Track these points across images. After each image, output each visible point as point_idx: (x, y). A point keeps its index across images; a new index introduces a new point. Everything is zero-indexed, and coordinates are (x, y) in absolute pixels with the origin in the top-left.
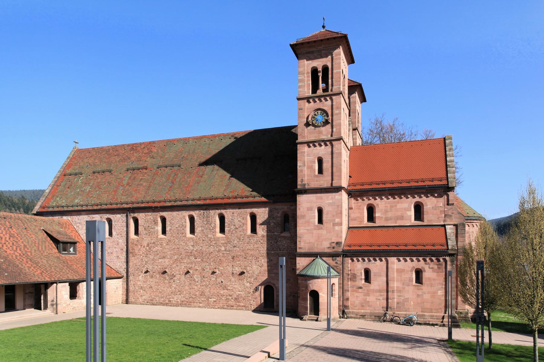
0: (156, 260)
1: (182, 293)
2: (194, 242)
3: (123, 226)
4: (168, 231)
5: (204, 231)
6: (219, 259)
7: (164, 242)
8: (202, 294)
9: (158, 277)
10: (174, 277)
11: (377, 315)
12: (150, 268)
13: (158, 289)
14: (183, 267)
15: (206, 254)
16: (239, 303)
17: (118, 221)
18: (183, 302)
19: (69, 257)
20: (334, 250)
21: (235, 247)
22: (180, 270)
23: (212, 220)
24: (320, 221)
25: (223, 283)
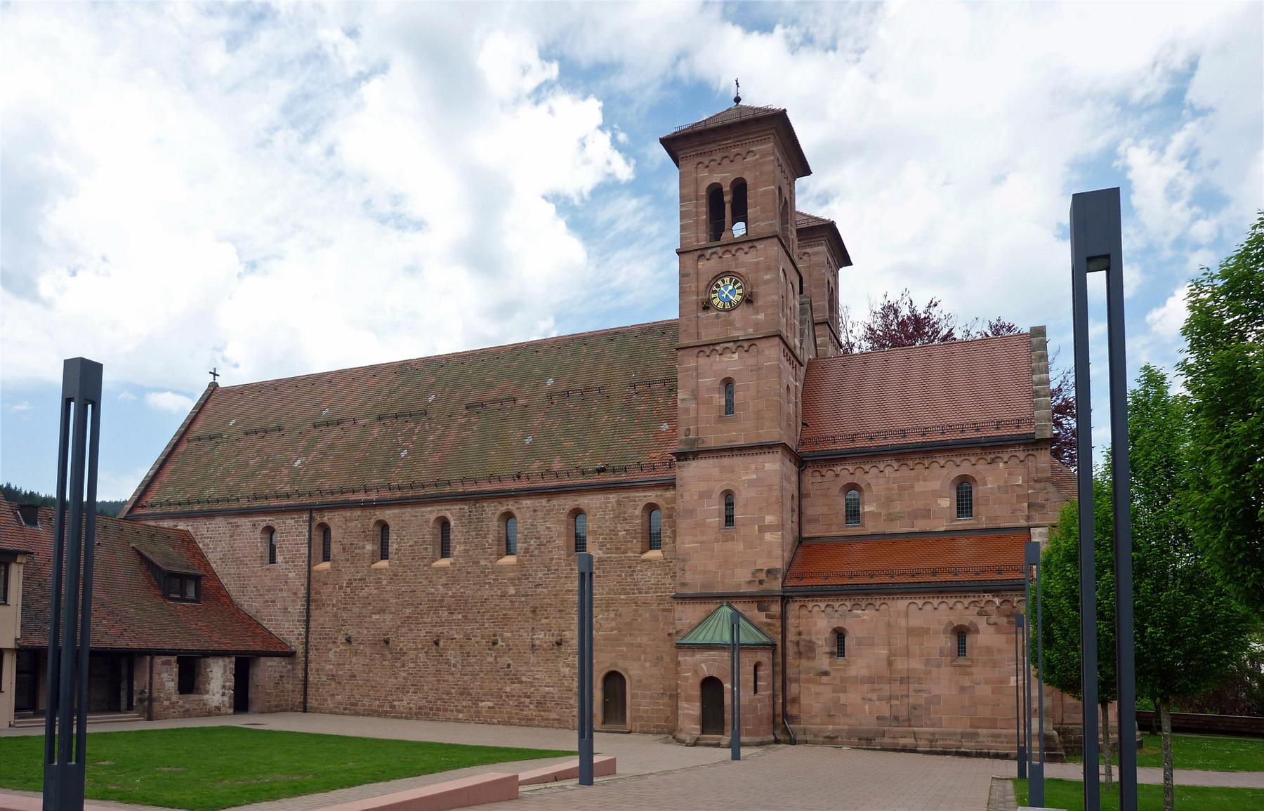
0: (365, 616)
1: (419, 689)
2: (449, 577)
3: (298, 544)
4: (392, 553)
5: (471, 553)
6: (505, 615)
7: (383, 577)
8: (464, 692)
9: (368, 654)
11: (864, 736)
12: (352, 632)
14: (422, 634)
15: (475, 602)
16: (547, 713)
17: (289, 533)
18: (421, 709)
19: (184, 605)
20: (762, 587)
21: (537, 586)
22: (415, 639)
23: (489, 527)
24: (729, 520)
25: (511, 669)
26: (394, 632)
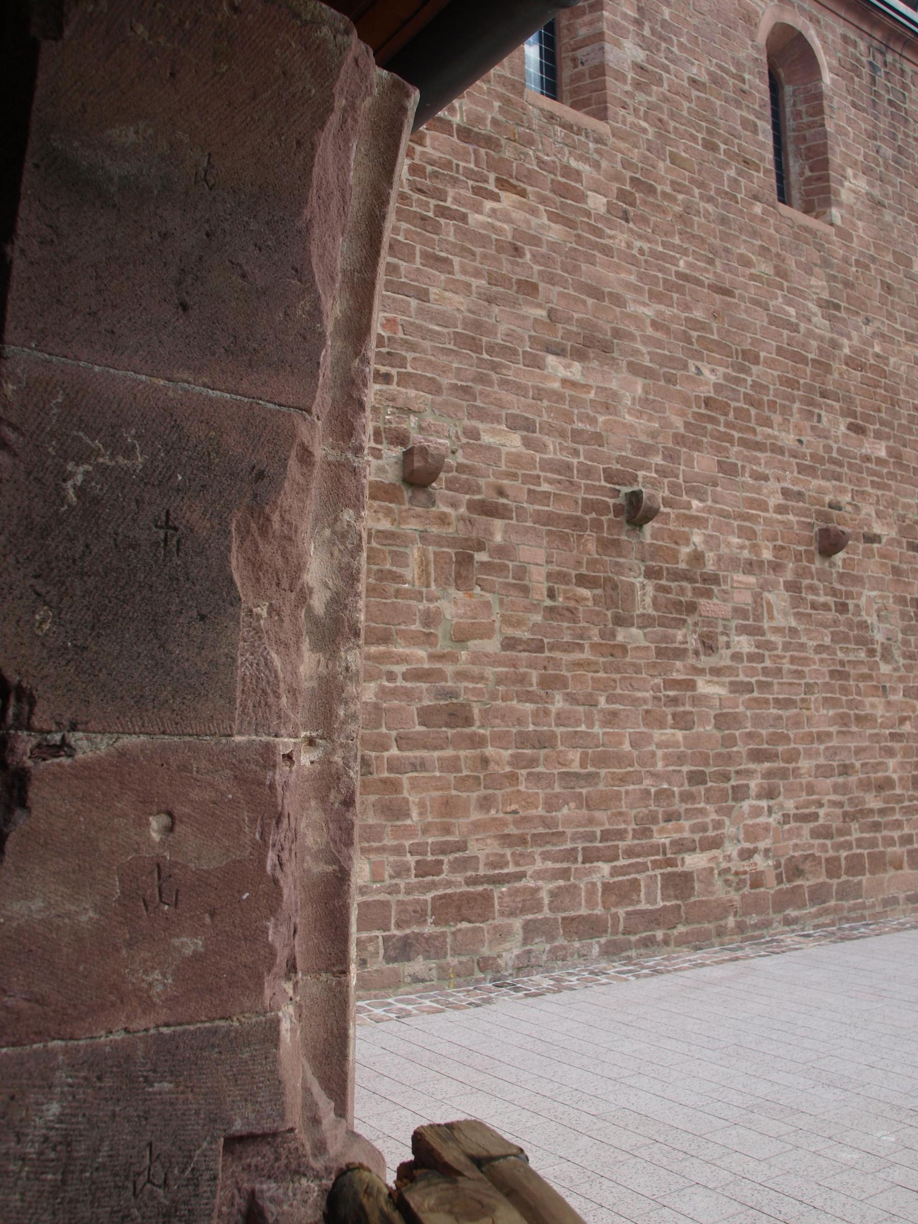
0: (509, 352)
9: (538, 578)
10: (708, 594)
13: (544, 741)
26: (662, 472)
